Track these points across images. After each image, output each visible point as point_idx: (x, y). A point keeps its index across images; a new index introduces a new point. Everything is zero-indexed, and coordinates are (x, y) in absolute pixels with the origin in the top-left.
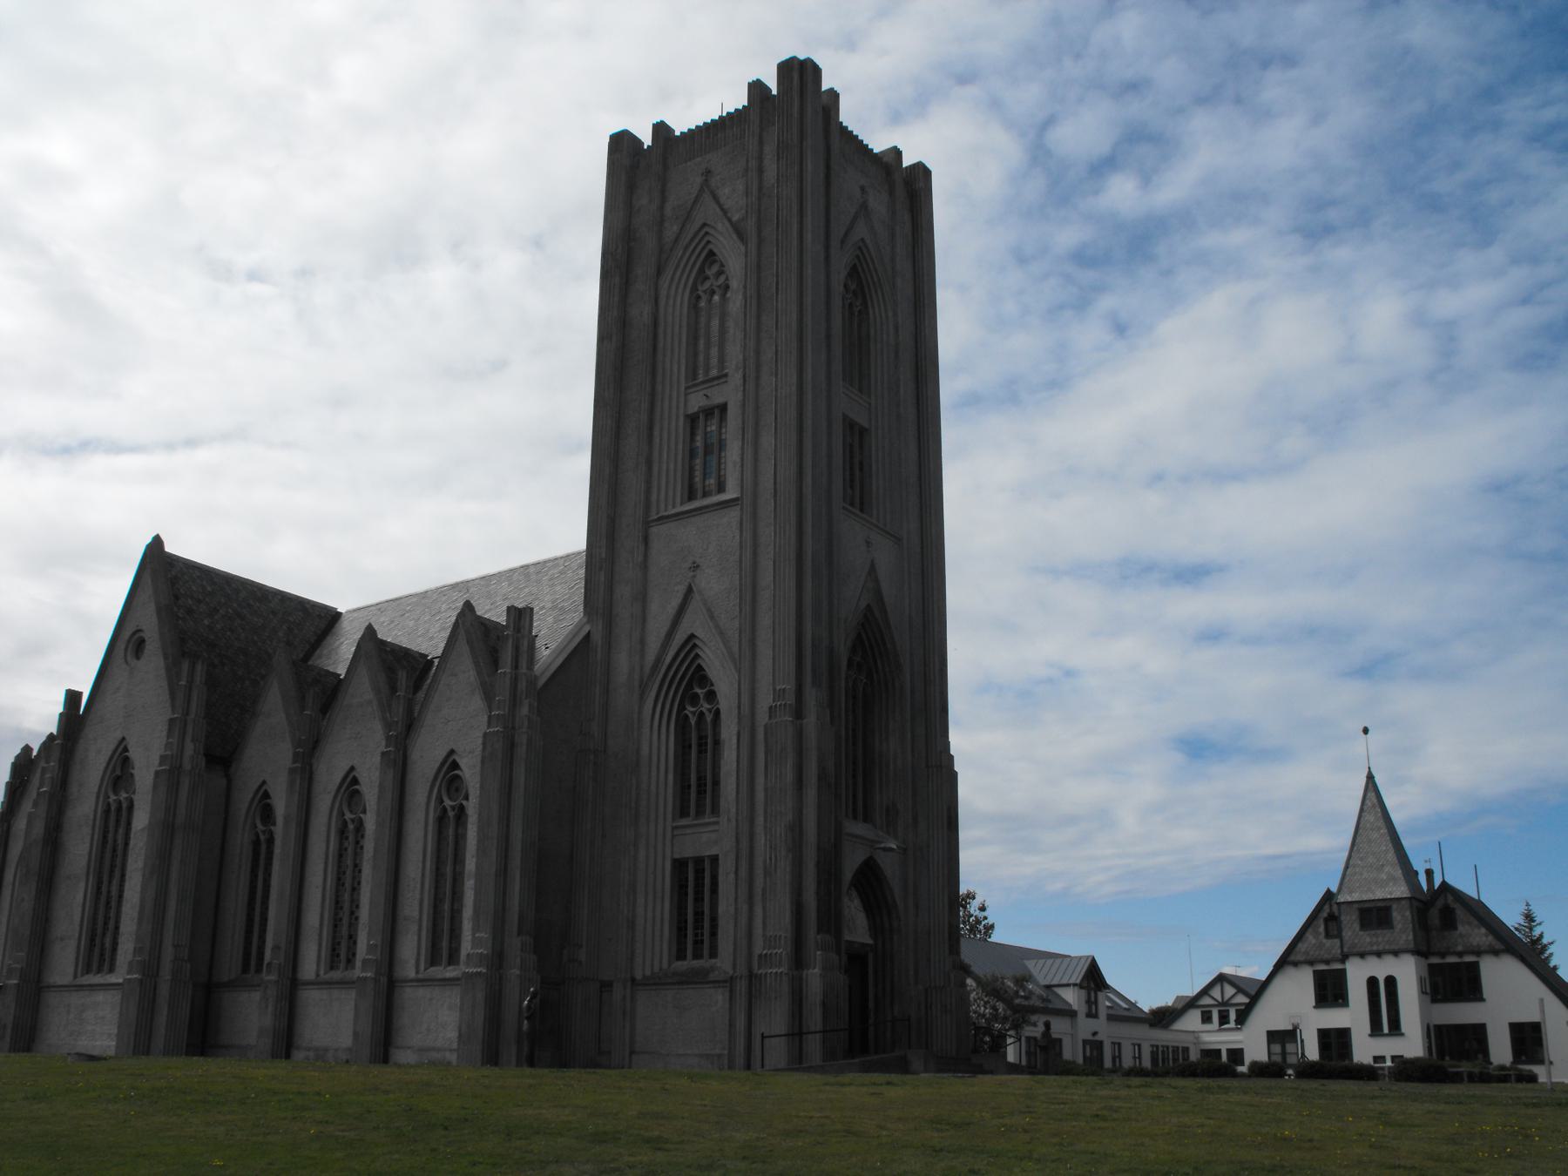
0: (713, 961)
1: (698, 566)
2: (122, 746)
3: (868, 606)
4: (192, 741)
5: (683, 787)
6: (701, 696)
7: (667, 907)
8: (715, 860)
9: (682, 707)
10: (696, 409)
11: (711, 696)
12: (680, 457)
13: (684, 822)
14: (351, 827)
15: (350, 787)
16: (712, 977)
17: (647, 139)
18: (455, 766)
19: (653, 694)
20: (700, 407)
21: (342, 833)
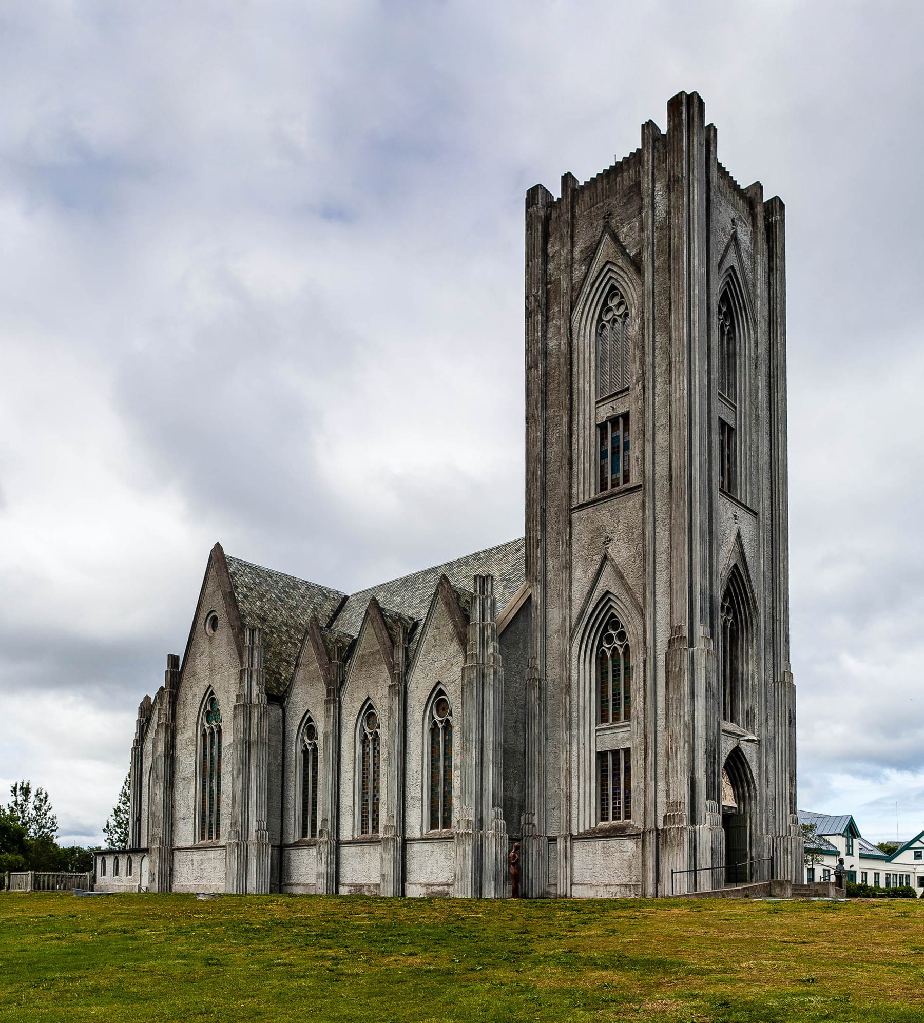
0: (628, 821)
6: (615, 636)
8: (627, 751)
9: (600, 645)
10: (604, 419)
11: (622, 636)
12: (593, 457)
13: (604, 726)
17: (557, 193)
18: (441, 692)
19: (580, 636)
20: (607, 417)
21: (364, 741)
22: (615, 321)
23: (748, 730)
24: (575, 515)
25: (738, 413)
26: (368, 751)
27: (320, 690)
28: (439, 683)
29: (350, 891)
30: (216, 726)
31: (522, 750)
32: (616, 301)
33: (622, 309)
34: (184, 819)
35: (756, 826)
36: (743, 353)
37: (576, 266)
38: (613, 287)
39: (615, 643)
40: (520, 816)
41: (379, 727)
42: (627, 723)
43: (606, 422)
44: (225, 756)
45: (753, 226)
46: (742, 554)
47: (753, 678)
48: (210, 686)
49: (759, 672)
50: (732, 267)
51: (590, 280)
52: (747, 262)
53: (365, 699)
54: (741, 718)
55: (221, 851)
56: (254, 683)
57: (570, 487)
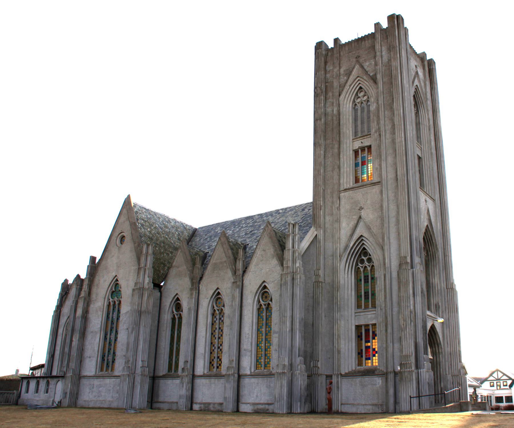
1: (363, 208)
2: (115, 279)
3: (427, 226)
4: (148, 277)
5: (358, 297)
6: (365, 260)
7: (353, 344)
9: (357, 264)
10: (357, 148)
11: (370, 260)
13: (359, 310)
14: (217, 312)
15: (217, 296)
16: (376, 373)
17: (331, 45)
18: (265, 287)
19: (345, 259)
20: (359, 147)
22: (362, 103)
23: (437, 315)
24: (342, 195)
25: (423, 150)
26: (215, 319)
27: (186, 282)
28: (264, 282)
29: (201, 407)
30: (118, 300)
31: (312, 323)
32: (362, 94)
33: (365, 98)
34: (90, 357)
35: (443, 370)
36: (423, 123)
37: (341, 77)
38: (361, 88)
39: (365, 264)
40: (310, 362)
41: (224, 306)
42: (374, 309)
43: (358, 149)
44: (123, 319)
45: (423, 69)
46: (430, 220)
47: (437, 286)
48: (116, 276)
49: (440, 283)
50: (417, 85)
51: (349, 83)
52: (423, 84)
53: (215, 289)
54: (433, 308)
55: (115, 379)
56: (146, 276)
57: (339, 179)
